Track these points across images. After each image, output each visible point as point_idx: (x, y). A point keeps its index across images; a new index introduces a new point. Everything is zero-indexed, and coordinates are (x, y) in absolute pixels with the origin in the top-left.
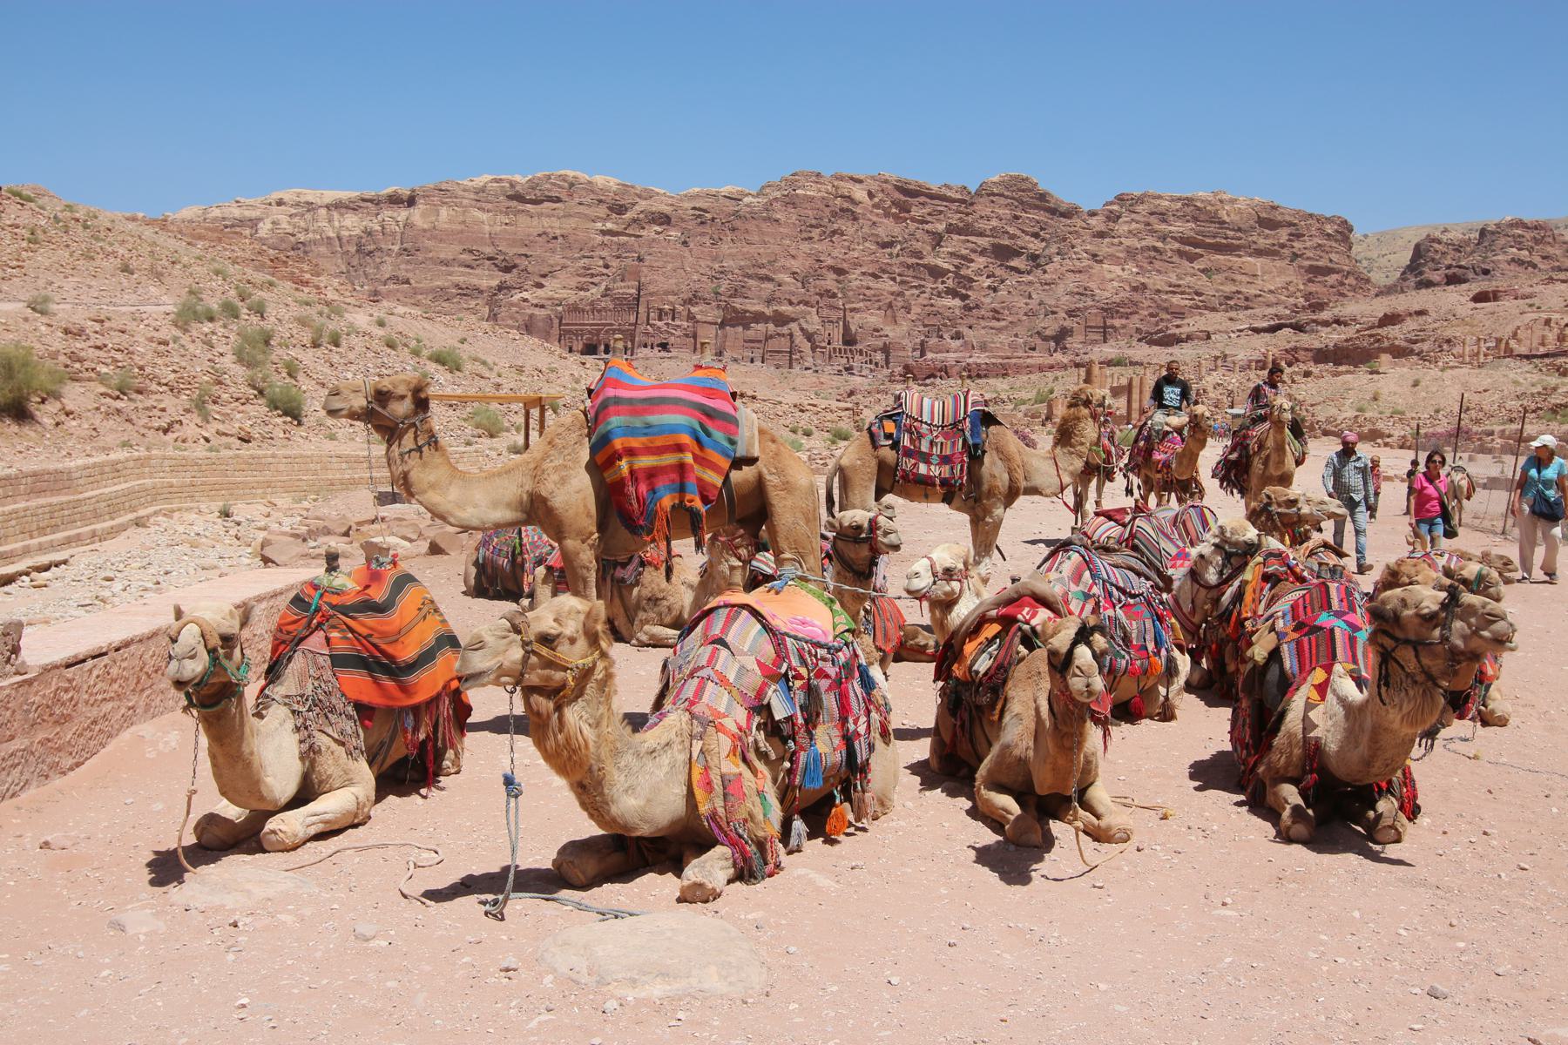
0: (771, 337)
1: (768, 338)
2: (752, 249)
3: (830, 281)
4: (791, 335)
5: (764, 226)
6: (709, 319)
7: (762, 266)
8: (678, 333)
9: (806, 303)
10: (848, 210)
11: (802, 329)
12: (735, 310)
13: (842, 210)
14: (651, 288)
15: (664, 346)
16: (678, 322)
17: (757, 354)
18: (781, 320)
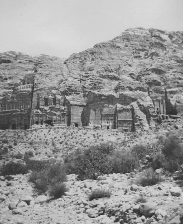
0: (120, 111)
1: (117, 112)
2: (105, 63)
3: (155, 76)
4: (133, 110)
5: (111, 50)
6: (78, 103)
7: (111, 71)
8: (58, 113)
9: (141, 89)
10: (159, 43)
11: (140, 105)
12: (96, 96)
13: (156, 43)
14: (41, 86)
15: (50, 122)
16: (58, 106)
17: (111, 124)
18: (125, 100)
